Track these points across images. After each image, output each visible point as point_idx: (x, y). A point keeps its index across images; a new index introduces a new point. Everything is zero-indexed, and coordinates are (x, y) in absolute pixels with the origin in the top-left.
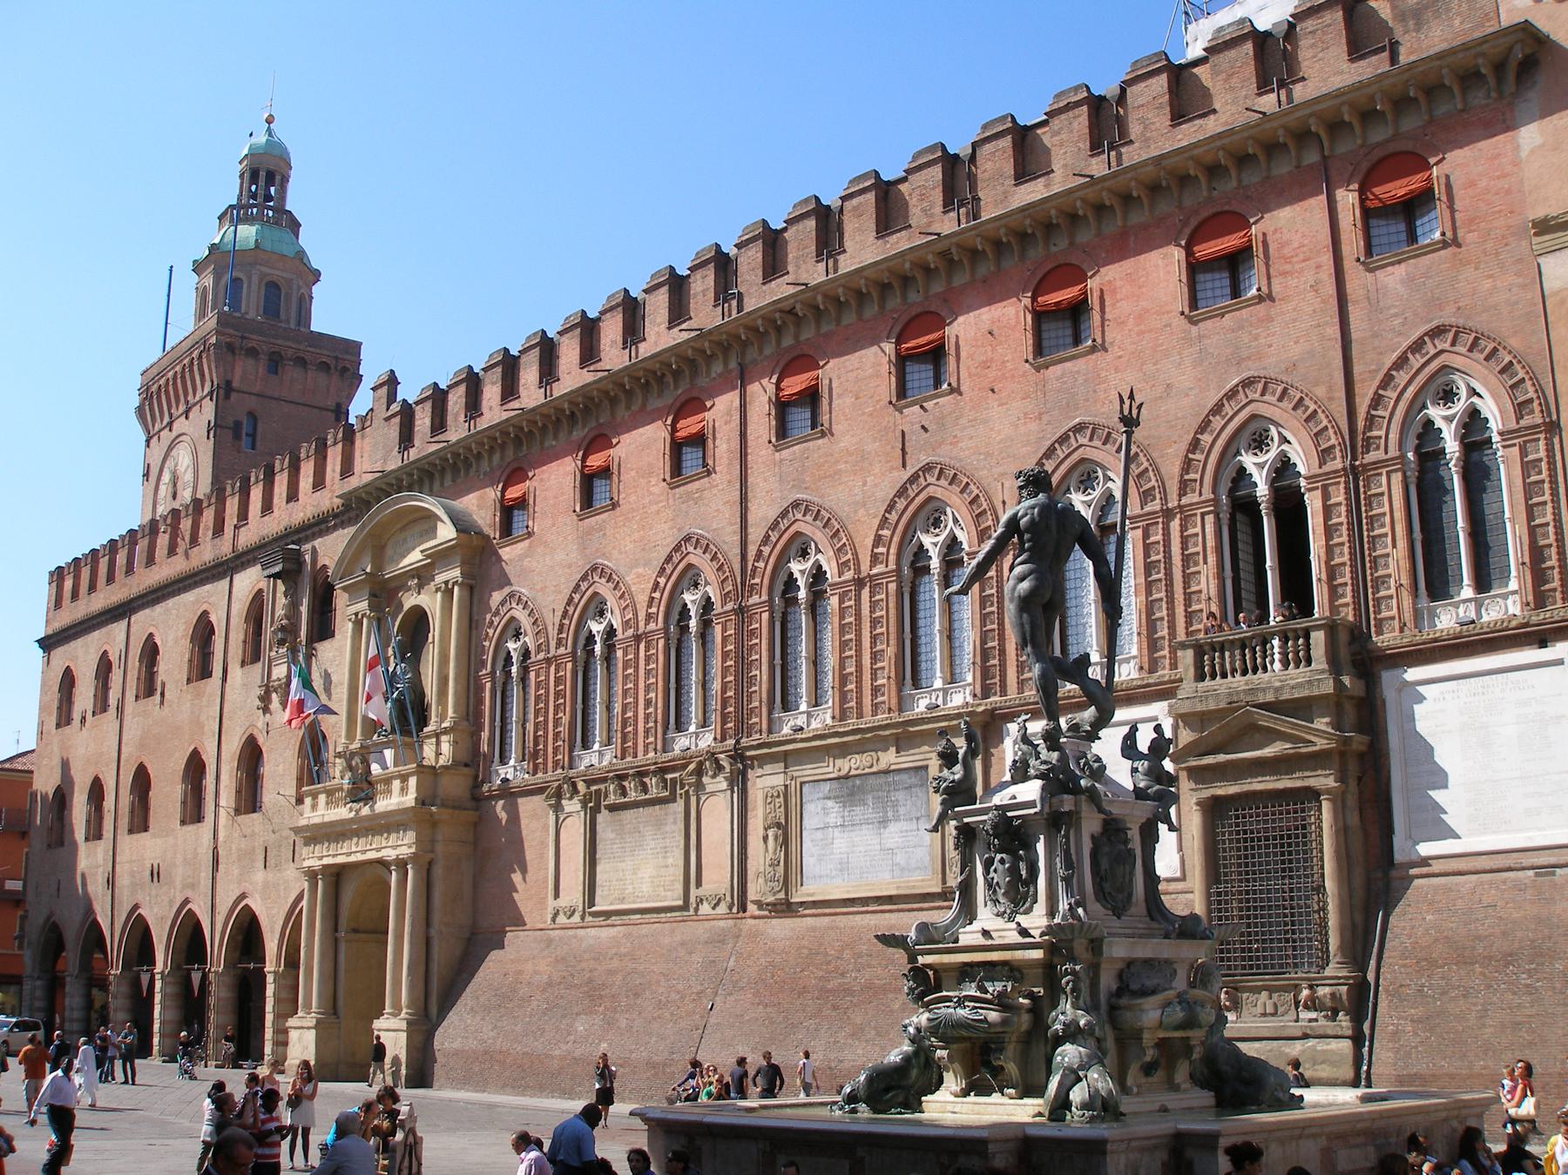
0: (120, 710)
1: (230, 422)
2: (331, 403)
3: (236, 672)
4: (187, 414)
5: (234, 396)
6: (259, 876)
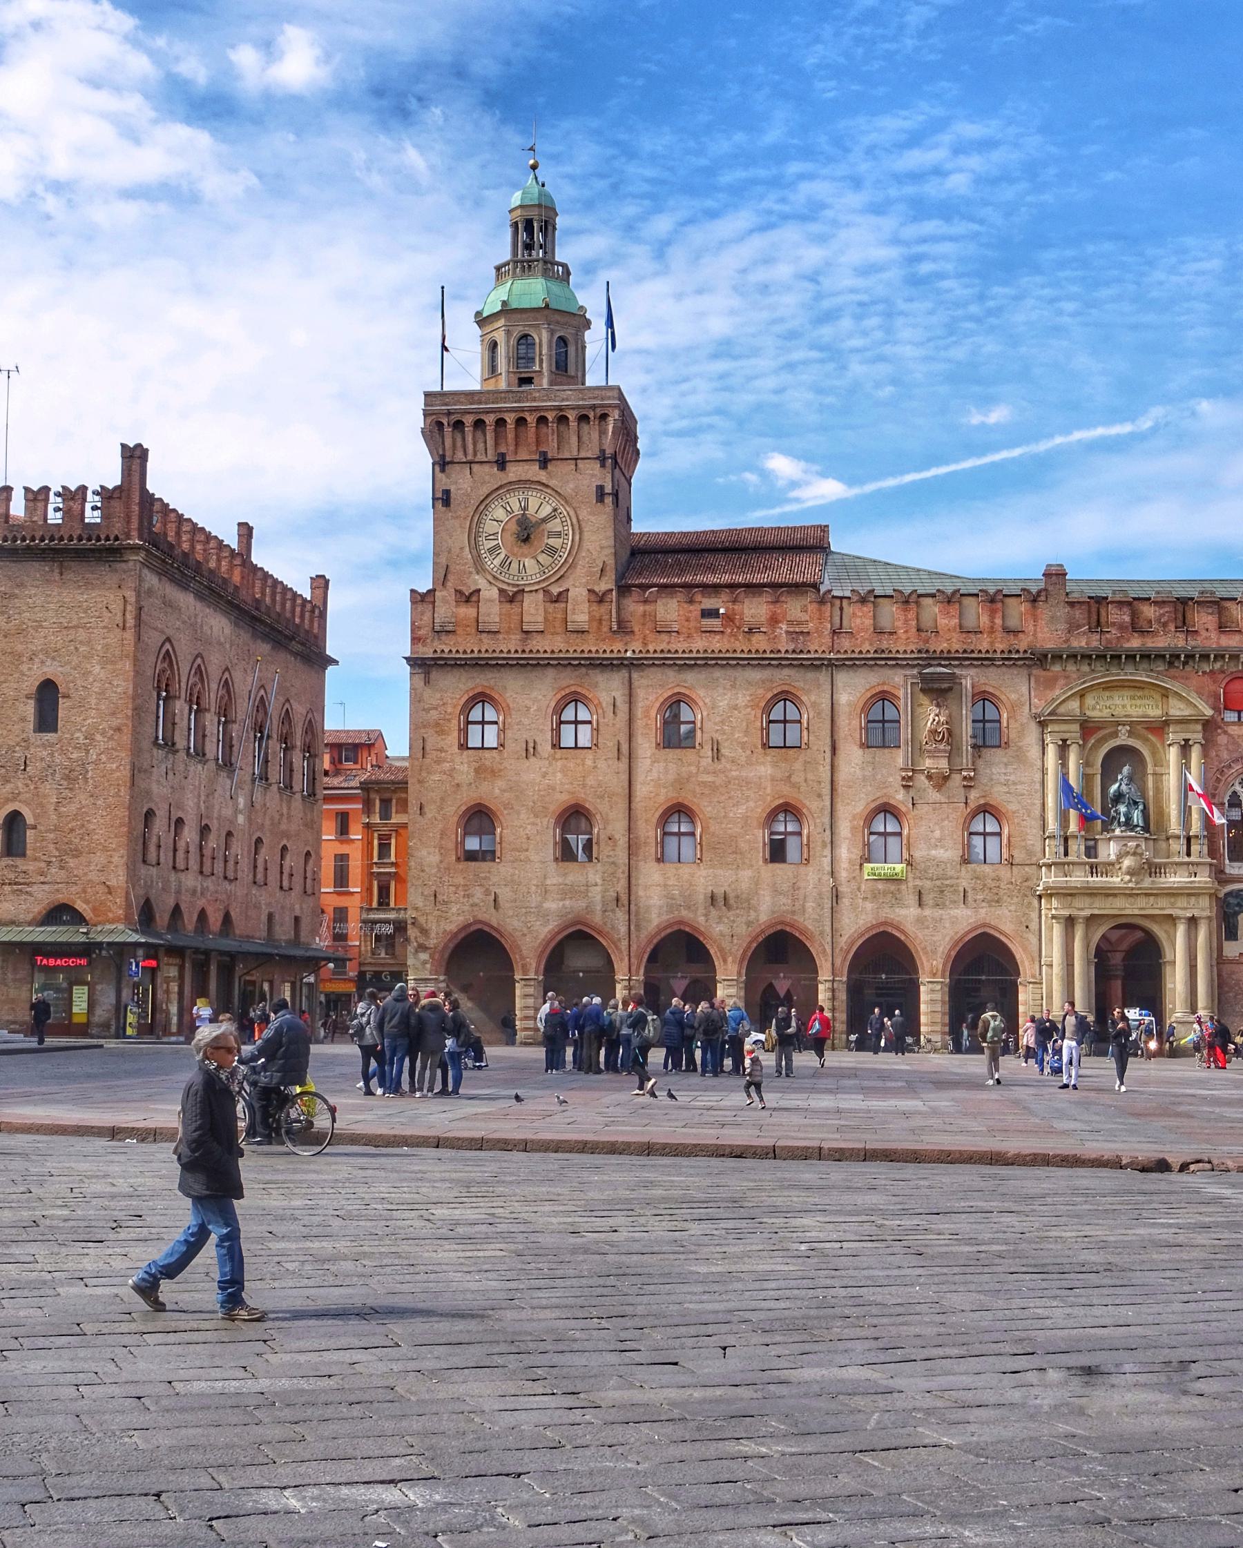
4: (544, 462)
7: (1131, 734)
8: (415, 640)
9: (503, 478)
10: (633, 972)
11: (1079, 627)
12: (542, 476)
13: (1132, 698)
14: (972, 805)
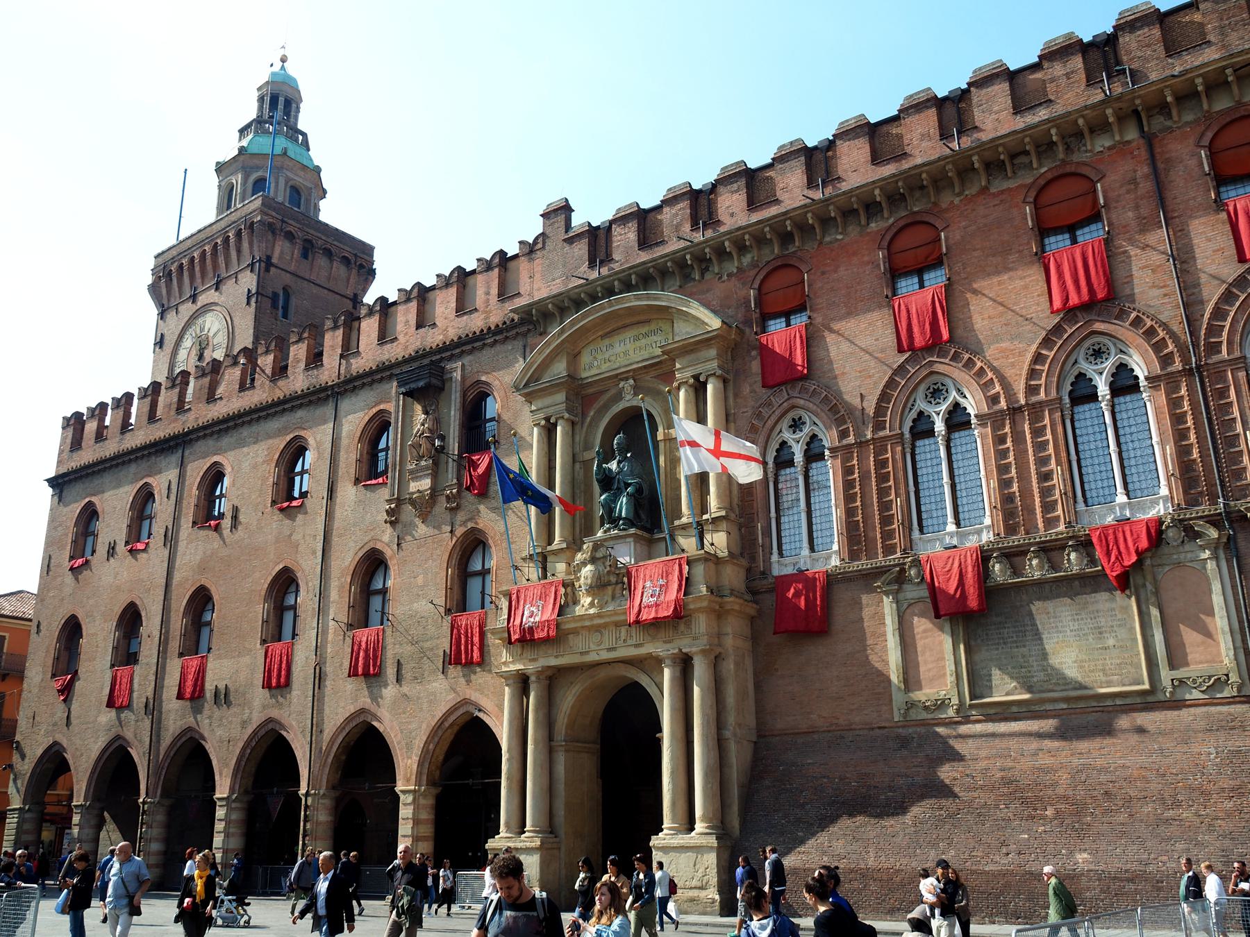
0: (170, 539)
1: (269, 292)
2: (349, 292)
3: (348, 492)
5: (273, 270)
7: (637, 390)
8: (59, 462)
9: (195, 308)
13: (637, 338)
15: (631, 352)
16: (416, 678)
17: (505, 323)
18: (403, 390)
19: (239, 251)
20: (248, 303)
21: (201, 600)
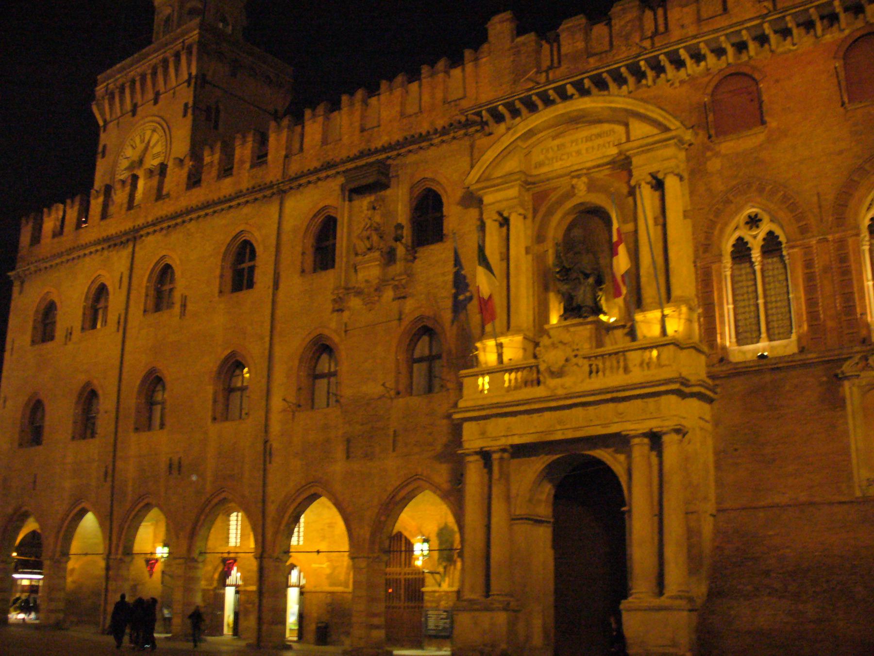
0: (123, 324)
6: (338, 467)
7: (592, 186)
10: (113, 550)
11: (526, 72)
12: (155, 109)
13: (588, 139)
14: (407, 321)
15: (584, 152)
16: (367, 456)
17: (451, 125)
18: (352, 186)
19: (177, 70)
20: (185, 115)
21: (154, 381)
